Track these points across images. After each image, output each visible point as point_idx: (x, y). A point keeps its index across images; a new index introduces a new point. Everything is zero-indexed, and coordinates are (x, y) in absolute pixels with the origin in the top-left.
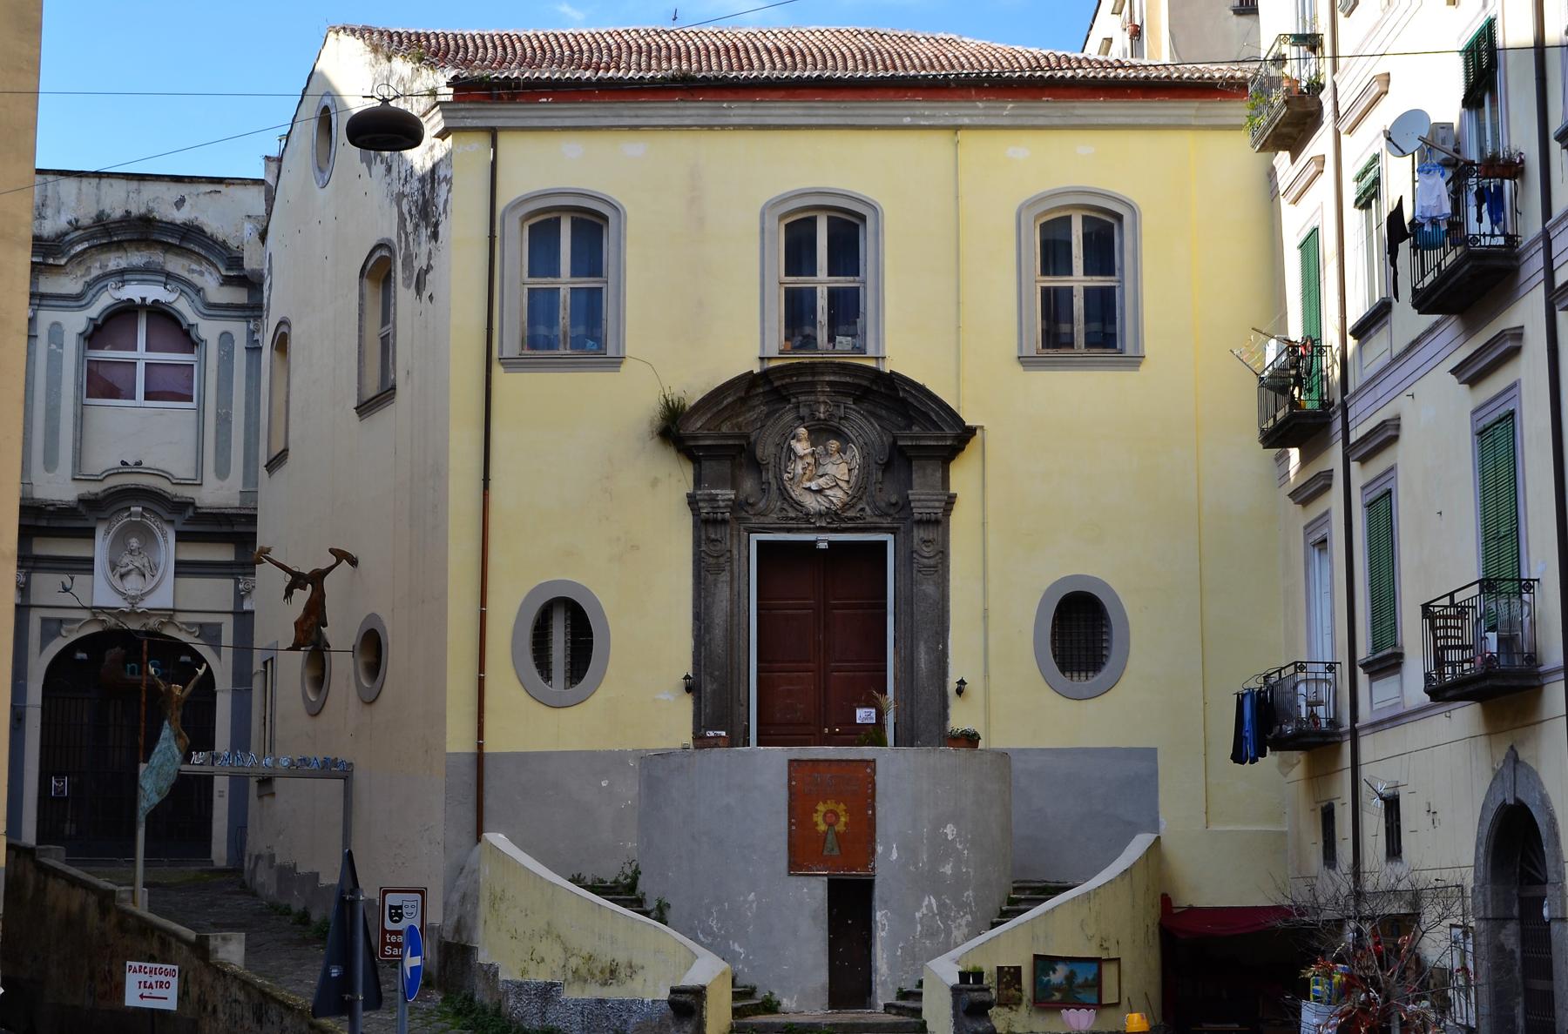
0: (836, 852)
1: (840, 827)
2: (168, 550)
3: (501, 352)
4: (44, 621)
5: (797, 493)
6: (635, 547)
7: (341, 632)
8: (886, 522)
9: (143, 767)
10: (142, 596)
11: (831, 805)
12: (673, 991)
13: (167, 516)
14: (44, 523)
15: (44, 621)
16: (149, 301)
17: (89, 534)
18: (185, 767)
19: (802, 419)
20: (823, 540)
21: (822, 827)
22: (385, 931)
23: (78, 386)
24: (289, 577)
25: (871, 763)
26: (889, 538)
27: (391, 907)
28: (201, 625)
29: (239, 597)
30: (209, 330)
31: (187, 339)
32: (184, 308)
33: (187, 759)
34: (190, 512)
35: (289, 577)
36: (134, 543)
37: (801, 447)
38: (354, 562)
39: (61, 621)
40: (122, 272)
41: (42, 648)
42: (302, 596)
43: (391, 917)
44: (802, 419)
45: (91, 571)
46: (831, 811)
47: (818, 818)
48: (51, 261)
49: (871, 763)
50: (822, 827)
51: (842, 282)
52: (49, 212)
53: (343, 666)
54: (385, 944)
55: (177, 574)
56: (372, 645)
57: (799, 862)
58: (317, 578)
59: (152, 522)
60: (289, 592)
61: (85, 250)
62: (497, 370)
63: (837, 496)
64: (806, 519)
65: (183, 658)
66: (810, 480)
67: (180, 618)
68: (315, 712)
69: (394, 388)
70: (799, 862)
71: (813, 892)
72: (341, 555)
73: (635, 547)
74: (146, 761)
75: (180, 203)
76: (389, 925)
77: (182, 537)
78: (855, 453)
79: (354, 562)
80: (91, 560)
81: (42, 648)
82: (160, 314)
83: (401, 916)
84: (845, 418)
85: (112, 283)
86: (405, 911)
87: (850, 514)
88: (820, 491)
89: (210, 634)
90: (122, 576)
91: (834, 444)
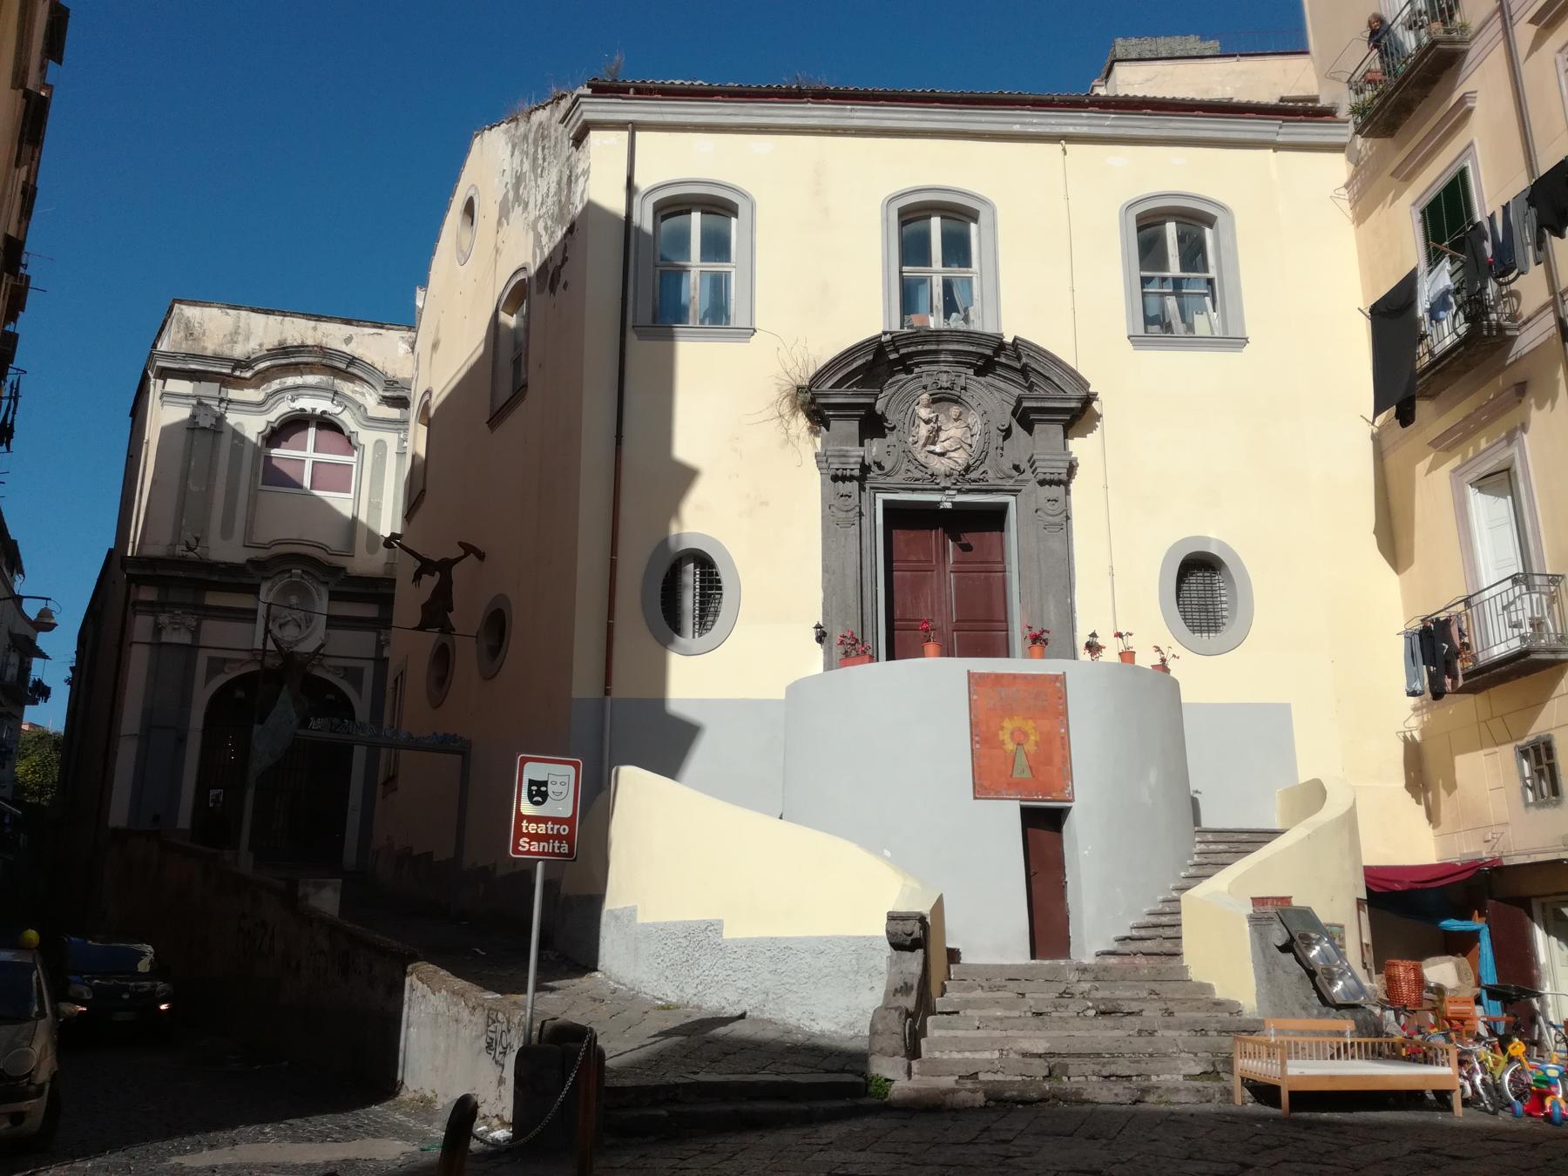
0: (1027, 774)
1: (1030, 747)
2: (323, 605)
3: (635, 320)
4: (211, 659)
5: (921, 457)
6: (765, 504)
7: (467, 615)
8: (1009, 484)
9: (257, 728)
10: (298, 642)
11: (1018, 722)
12: (893, 918)
13: (323, 579)
14: (215, 578)
15: (211, 659)
16: (318, 412)
17: (254, 590)
18: (301, 732)
19: (925, 387)
20: (946, 501)
21: (1010, 746)
22: (520, 817)
23: (254, 473)
24: (418, 564)
25: (1060, 679)
26: (1011, 499)
27: (531, 783)
28: (345, 668)
29: (380, 647)
30: (366, 437)
31: (350, 445)
32: (347, 419)
33: (304, 723)
34: (342, 576)
35: (418, 564)
36: (294, 600)
37: (924, 413)
38: (481, 556)
39: (225, 660)
40: (297, 387)
41: (207, 682)
42: (430, 582)
43: (531, 797)
44: (925, 387)
45: (254, 621)
46: (1019, 729)
47: (1005, 736)
48: (237, 373)
49: (1060, 679)
50: (1010, 746)
51: (955, 272)
52: (241, 338)
53: (466, 653)
54: (519, 834)
55: (328, 626)
56: (497, 624)
57: (984, 788)
58: (445, 566)
59: (308, 582)
60: (417, 577)
61: (268, 369)
62: (631, 337)
63: (961, 457)
64: (932, 481)
65: (329, 696)
66: (934, 443)
67: (327, 662)
68: (437, 704)
69: (525, 386)
70: (984, 788)
71: (1006, 816)
72: (468, 549)
73: (765, 504)
74: (261, 722)
75: (348, 340)
76: (527, 808)
77: (334, 596)
78: (974, 419)
79: (481, 556)
80: (255, 612)
81: (207, 682)
82: (327, 424)
83: (545, 796)
84: (965, 388)
85: (288, 395)
86: (551, 789)
87: (973, 475)
88: (942, 455)
89: (354, 676)
90: (281, 626)
91: (954, 410)
